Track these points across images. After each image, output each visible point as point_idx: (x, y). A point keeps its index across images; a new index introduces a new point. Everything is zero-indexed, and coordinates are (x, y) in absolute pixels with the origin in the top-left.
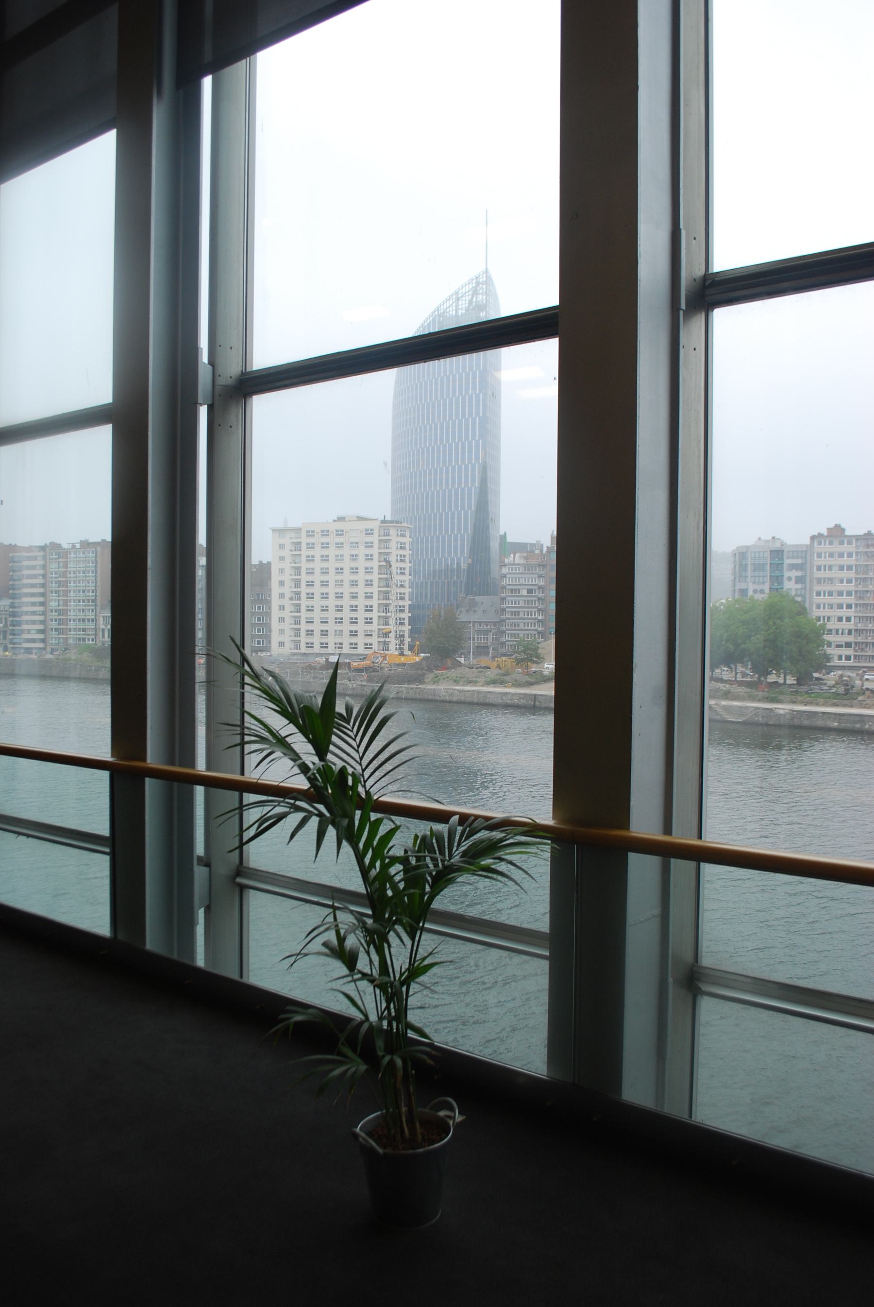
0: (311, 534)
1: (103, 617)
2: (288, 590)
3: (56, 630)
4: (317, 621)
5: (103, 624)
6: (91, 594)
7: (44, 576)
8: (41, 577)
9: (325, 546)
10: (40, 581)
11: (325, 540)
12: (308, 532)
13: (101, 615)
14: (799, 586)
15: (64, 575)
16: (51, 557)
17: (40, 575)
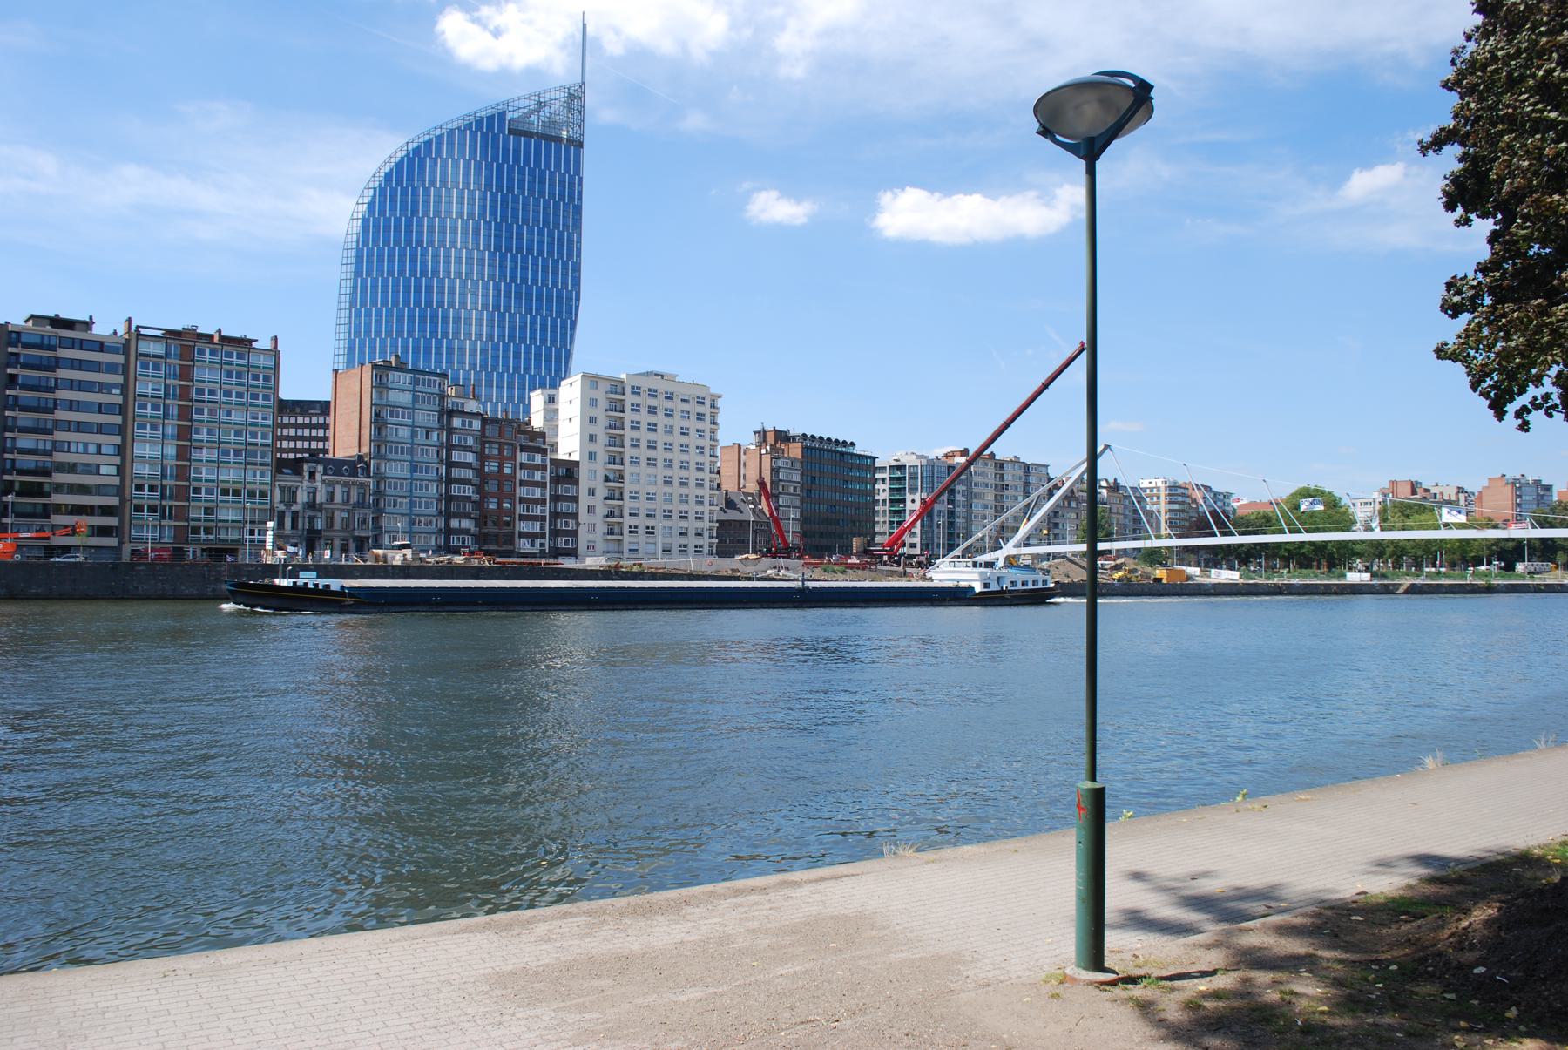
0: (636, 391)
1: (282, 489)
2: (600, 467)
3: (152, 509)
4: (643, 513)
5: (281, 502)
6: (259, 440)
7: (124, 388)
8: (118, 391)
9: (653, 411)
10: (115, 397)
11: (653, 402)
12: (633, 387)
13: (277, 483)
14: (964, 499)
15: (184, 393)
16: (141, 350)
17: (115, 386)
